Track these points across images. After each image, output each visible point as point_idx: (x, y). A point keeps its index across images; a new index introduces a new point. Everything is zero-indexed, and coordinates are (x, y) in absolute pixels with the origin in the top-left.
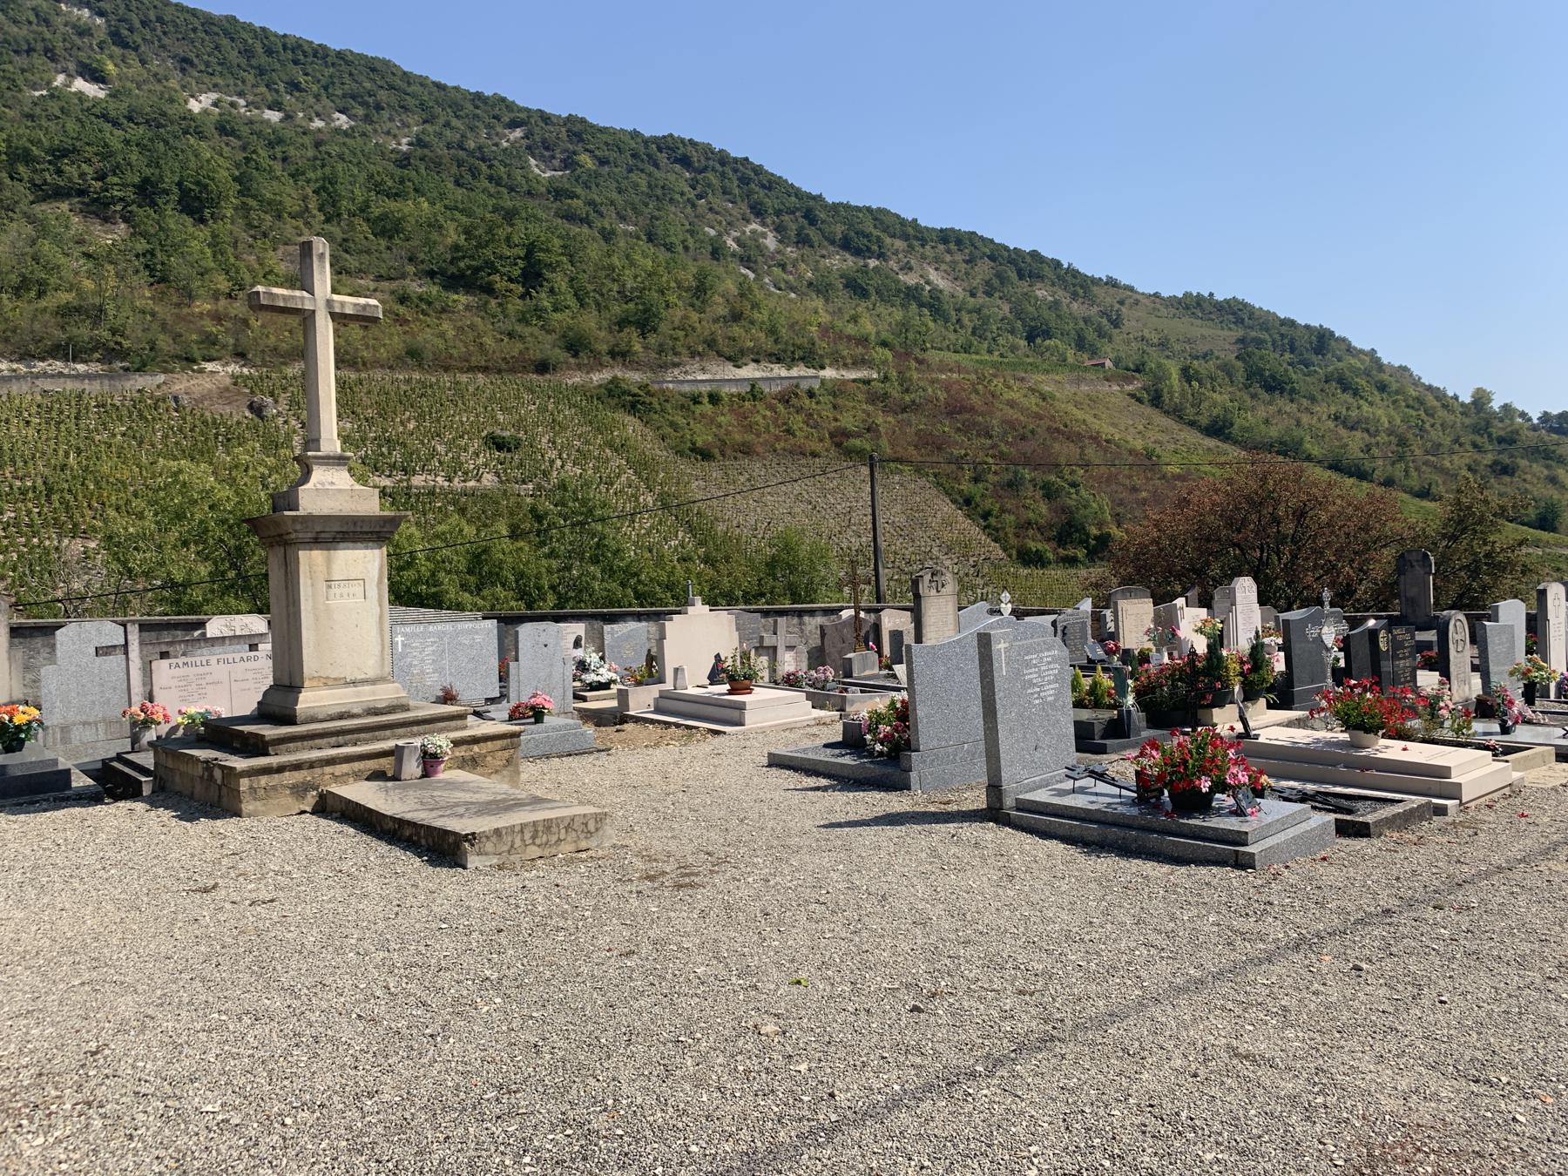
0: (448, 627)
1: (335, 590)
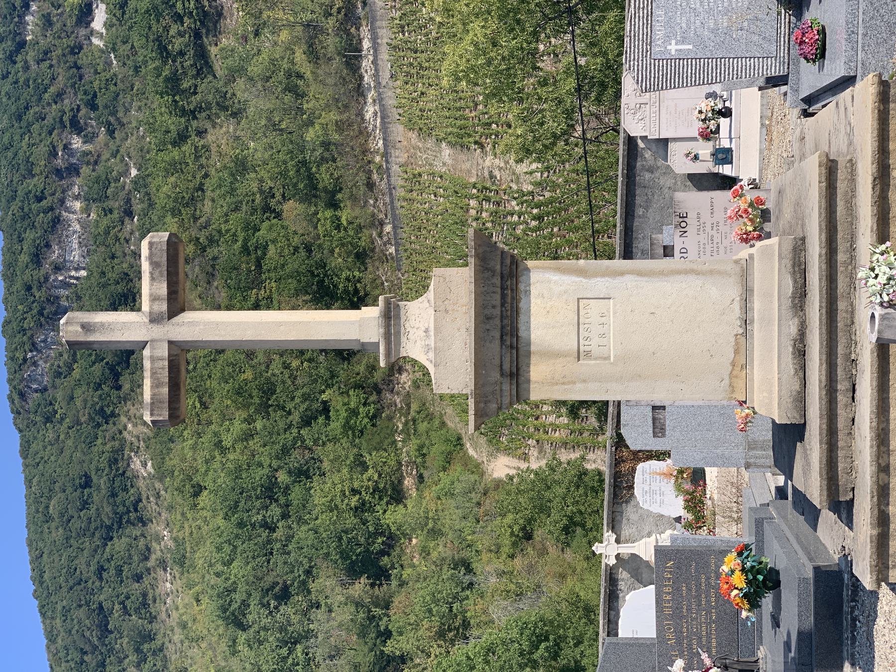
1: (593, 345)
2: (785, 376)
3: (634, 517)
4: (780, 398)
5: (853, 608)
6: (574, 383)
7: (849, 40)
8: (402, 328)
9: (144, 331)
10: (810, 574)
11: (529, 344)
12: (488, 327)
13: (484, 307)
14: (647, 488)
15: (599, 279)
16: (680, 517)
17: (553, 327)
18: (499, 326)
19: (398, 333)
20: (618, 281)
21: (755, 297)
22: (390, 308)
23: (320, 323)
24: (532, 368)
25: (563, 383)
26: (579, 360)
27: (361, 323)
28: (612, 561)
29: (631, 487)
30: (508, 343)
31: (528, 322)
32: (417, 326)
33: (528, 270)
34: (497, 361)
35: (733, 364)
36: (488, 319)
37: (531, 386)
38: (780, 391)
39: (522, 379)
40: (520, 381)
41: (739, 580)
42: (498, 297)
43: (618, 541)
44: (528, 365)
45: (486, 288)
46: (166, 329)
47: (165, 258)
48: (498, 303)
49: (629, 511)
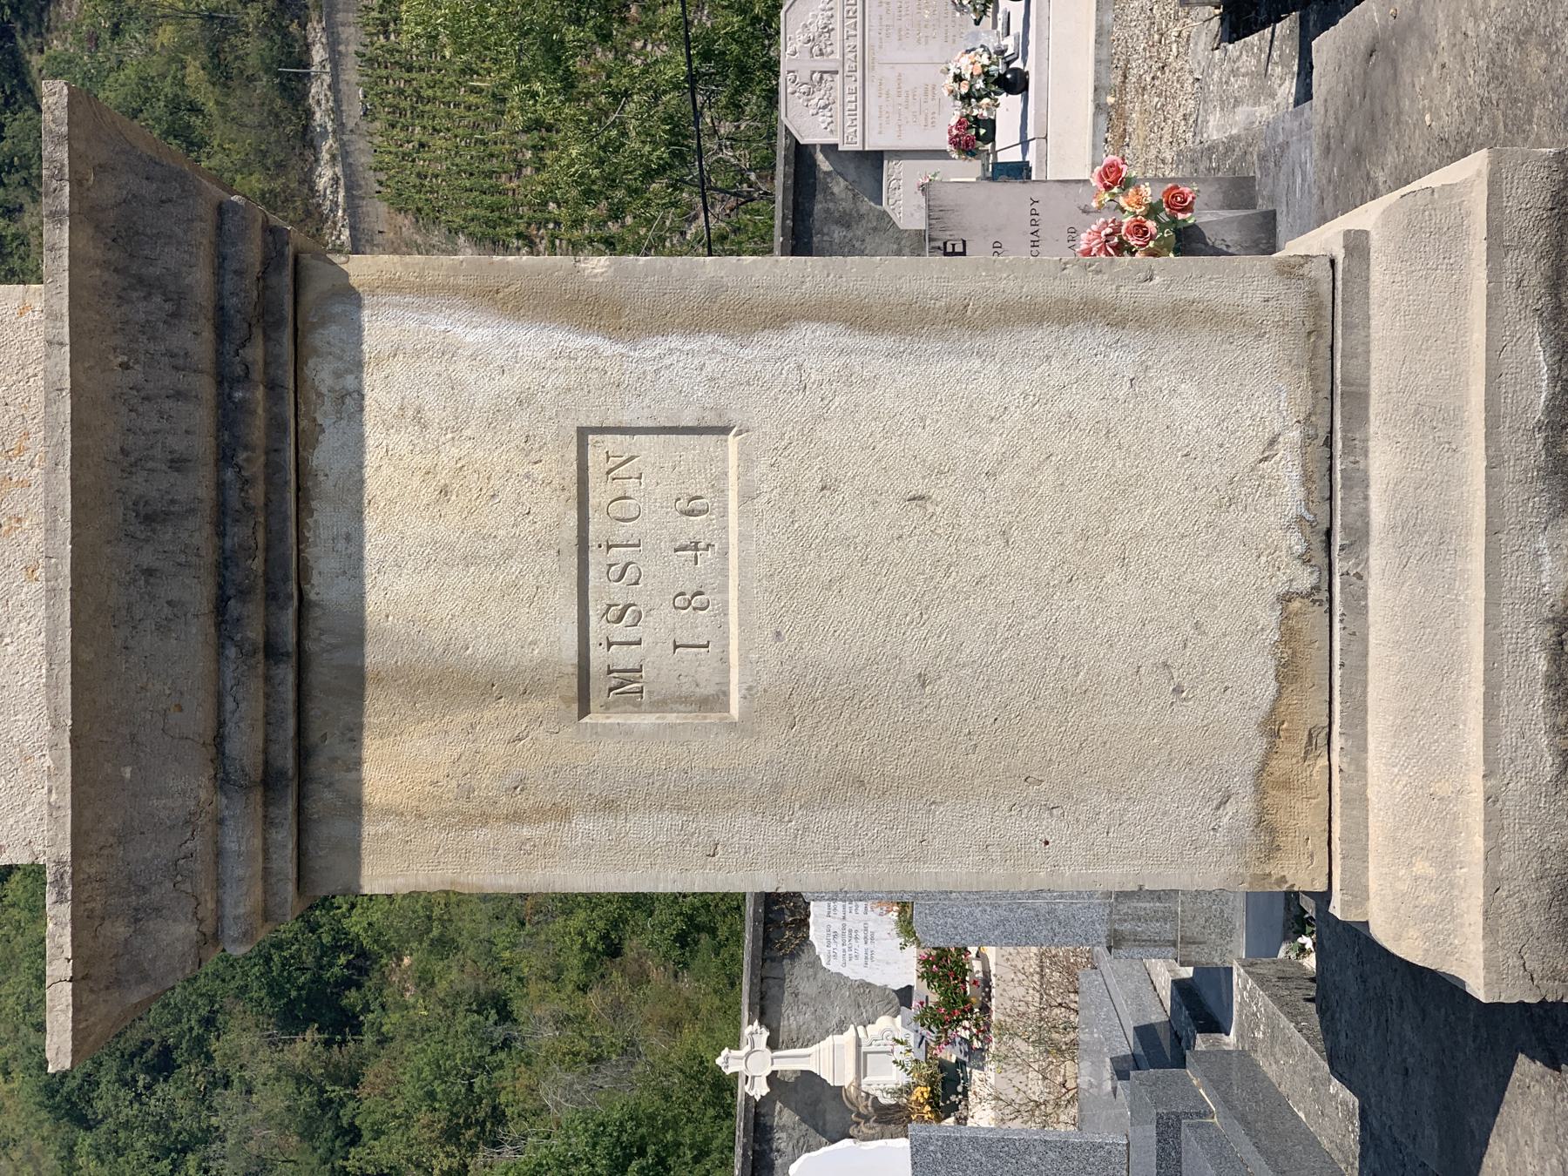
1: (650, 642)
2: (1519, 785)
3: (807, 988)
4: (1493, 886)
6: (564, 814)
11: (355, 635)
12: (147, 558)
13: (130, 461)
14: (836, 926)
15: (675, 341)
16: (910, 988)
17: (468, 560)
18: (209, 556)
20: (759, 352)
21: (1375, 425)
24: (373, 750)
25: (516, 817)
26: (584, 711)
28: (760, 1090)
29: (803, 923)
30: (254, 633)
31: (353, 539)
33: (350, 296)
34: (198, 720)
35: (1272, 727)
36: (149, 519)
37: (369, 830)
38: (1492, 853)
39: (323, 799)
40: (315, 808)
42: (201, 417)
43: (773, 1044)
44: (353, 735)
45: (137, 374)
48: (203, 445)
49: (798, 978)
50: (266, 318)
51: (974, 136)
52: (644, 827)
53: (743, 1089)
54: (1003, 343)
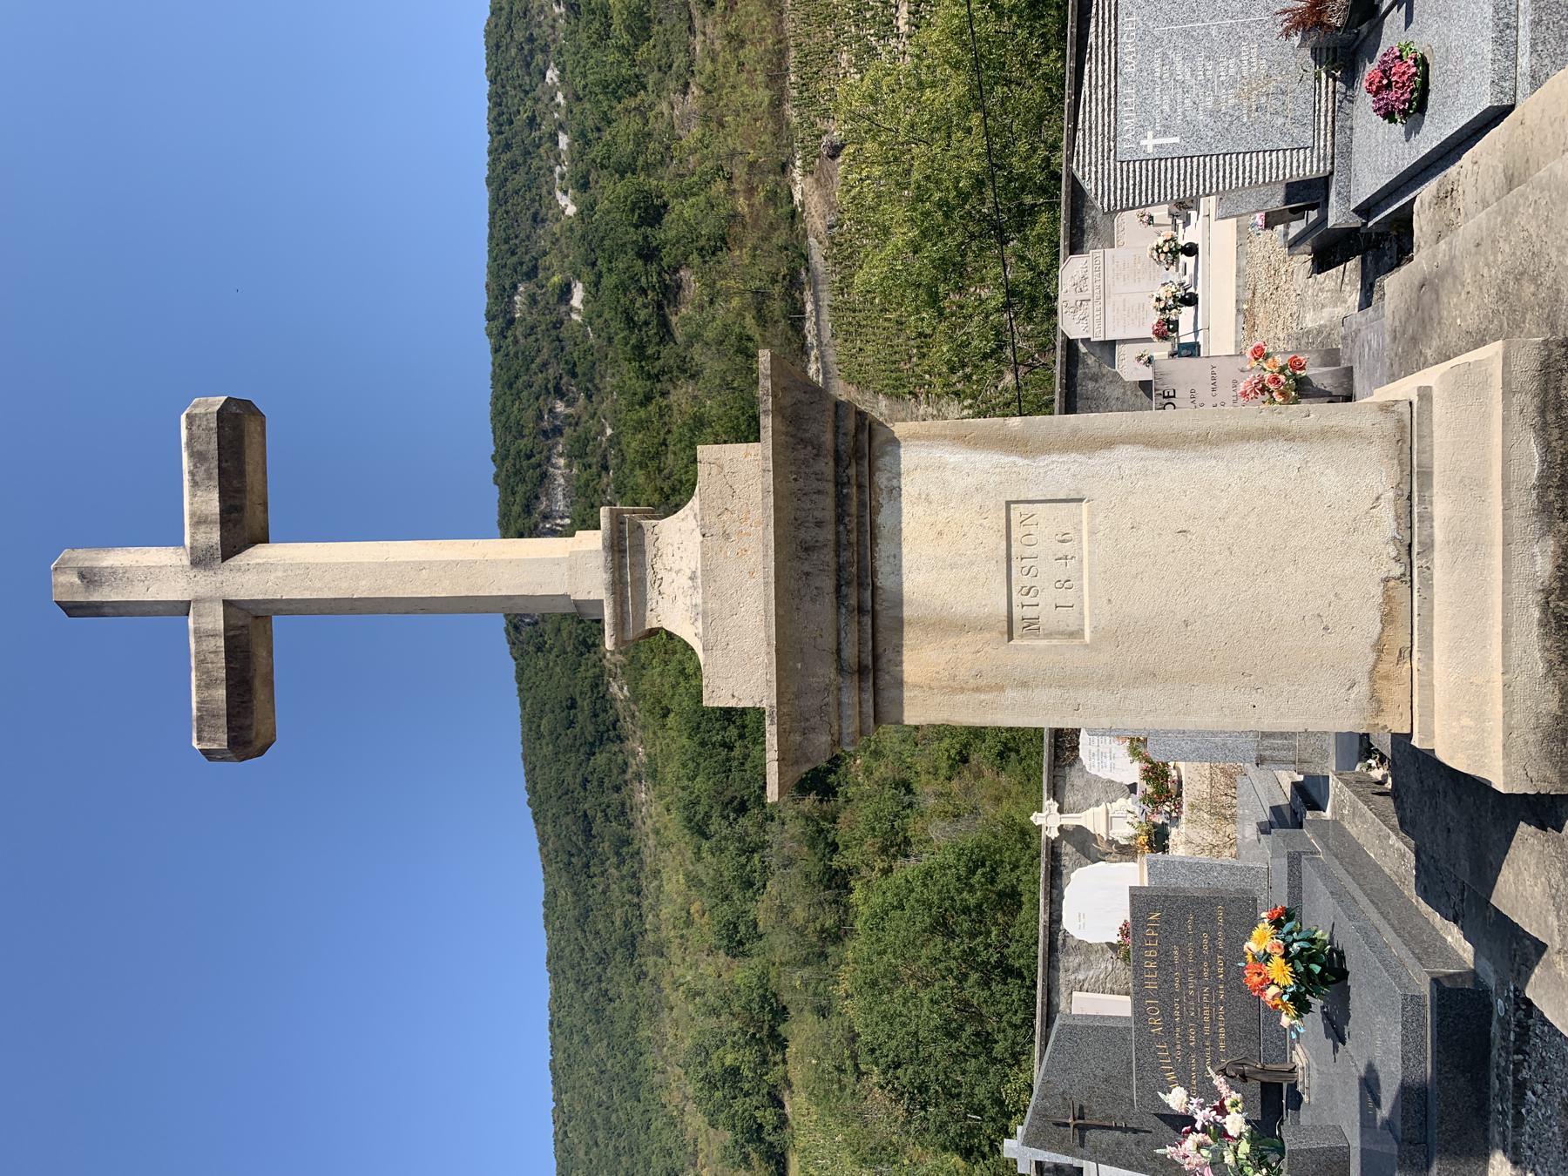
0: (1128, 25)
1: (1044, 604)
2: (1523, 678)
3: (1079, 782)
4: (1508, 731)
5: (1518, 1066)
6: (1002, 688)
7: (1499, 41)
8: (649, 572)
9: (183, 583)
10: (1425, 989)
11: (899, 603)
12: (806, 568)
13: (798, 523)
14: (1094, 750)
15: (1055, 457)
16: (1135, 784)
17: (952, 566)
18: (833, 566)
19: (640, 583)
20: (1100, 461)
21: (1436, 488)
22: (622, 531)
23: (494, 563)
24: (907, 655)
25: (977, 689)
26: (1011, 638)
27: (573, 564)
28: (1054, 834)
29: (1076, 748)
30: (853, 602)
31: (897, 556)
32: (676, 567)
33: (895, 442)
34: (829, 642)
35: (1379, 648)
36: (806, 550)
37: (906, 694)
38: (1508, 715)
39: (885, 679)
40: (881, 684)
41: (1279, 971)
42: (829, 502)
43: (1060, 811)
46: (220, 578)
47: (214, 445)
48: (829, 515)
49: (1073, 776)
50: (857, 454)
51: (1166, 329)
52: (1042, 696)
53: (1044, 833)
54: (1228, 451)
